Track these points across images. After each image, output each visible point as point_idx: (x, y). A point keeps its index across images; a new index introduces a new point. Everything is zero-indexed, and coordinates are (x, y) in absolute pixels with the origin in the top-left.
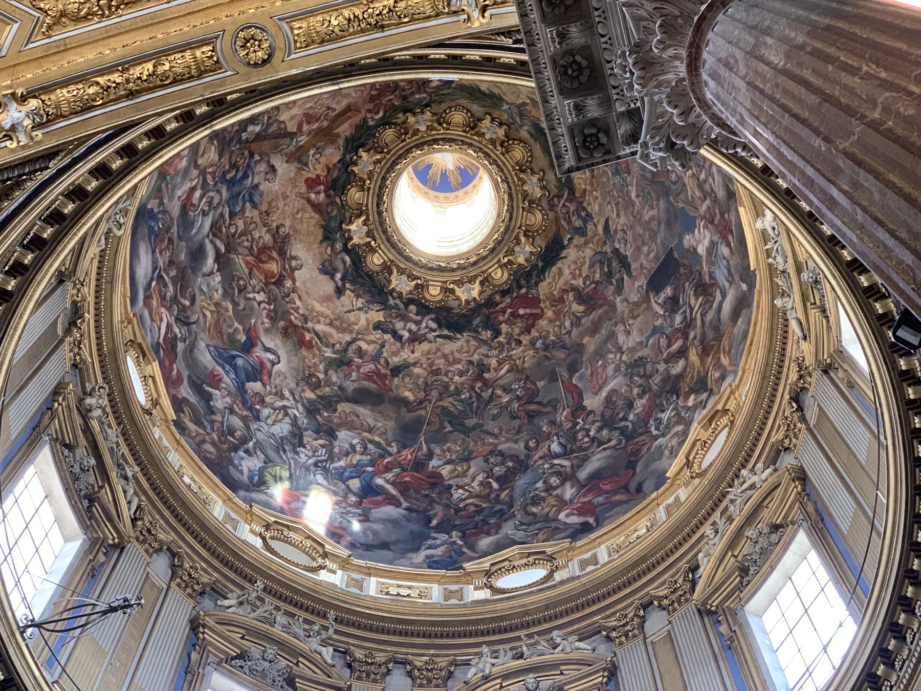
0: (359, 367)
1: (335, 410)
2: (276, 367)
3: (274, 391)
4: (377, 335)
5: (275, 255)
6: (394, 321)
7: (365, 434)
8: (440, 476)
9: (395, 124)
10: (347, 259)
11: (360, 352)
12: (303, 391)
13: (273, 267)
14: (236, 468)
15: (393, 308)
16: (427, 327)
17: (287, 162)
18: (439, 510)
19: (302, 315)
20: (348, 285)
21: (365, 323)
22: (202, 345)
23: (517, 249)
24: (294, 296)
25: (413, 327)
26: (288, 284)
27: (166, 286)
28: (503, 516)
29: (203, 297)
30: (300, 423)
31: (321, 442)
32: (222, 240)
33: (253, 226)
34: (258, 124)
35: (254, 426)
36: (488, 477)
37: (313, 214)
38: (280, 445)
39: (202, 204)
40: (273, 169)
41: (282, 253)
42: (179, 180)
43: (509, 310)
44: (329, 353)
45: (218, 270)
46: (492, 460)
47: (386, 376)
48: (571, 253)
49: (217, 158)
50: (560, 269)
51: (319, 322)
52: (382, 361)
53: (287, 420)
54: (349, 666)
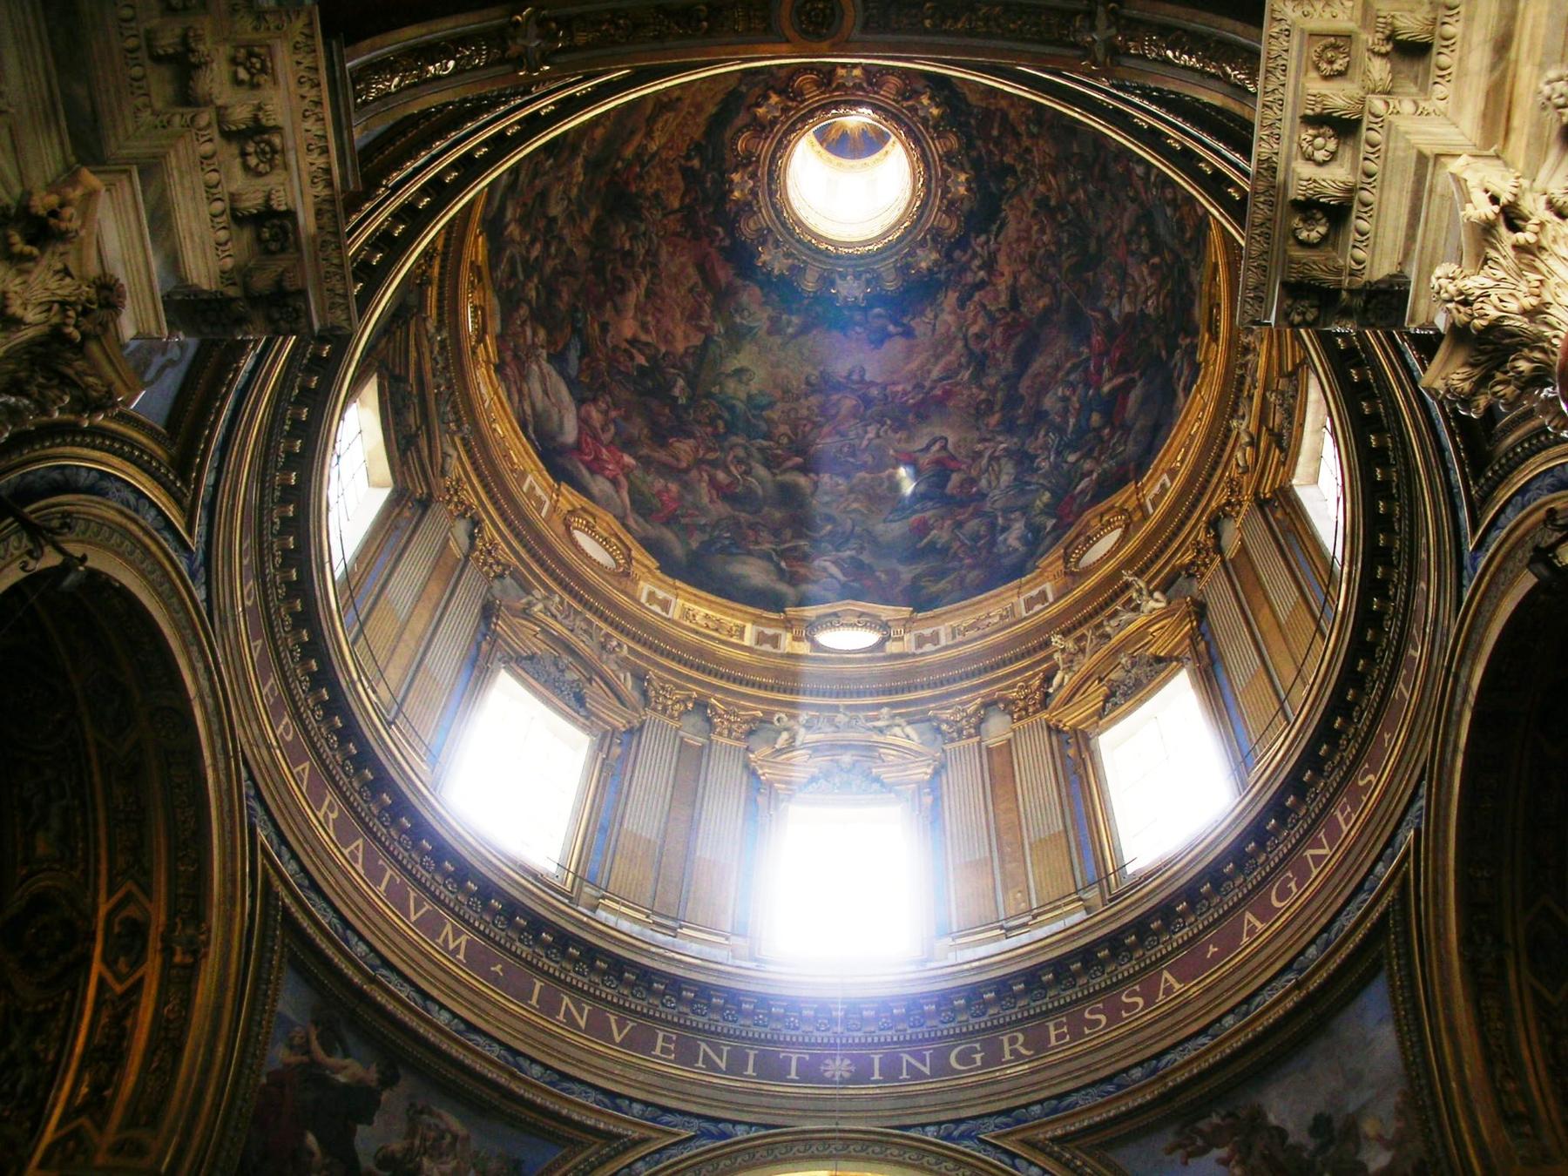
0: (994, 346)
1: (1022, 398)
2: (950, 446)
3: (969, 461)
4: (971, 306)
5: (835, 397)
7: (1060, 375)
8: (1129, 314)
9: (737, 214)
10: (877, 310)
11: (979, 337)
12: (987, 425)
13: (848, 403)
14: (1008, 554)
17: (738, 352)
18: (1156, 340)
19: (914, 388)
20: (905, 321)
22: (880, 528)
23: (921, 113)
24: (890, 389)
25: (977, 262)
26: (874, 392)
27: (795, 548)
28: (1184, 274)
29: (835, 505)
30: (1013, 448)
31: (1042, 433)
32: (788, 459)
33: (792, 416)
34: (676, 381)
35: (987, 507)
36: (1147, 262)
37: (811, 336)
38: (1020, 484)
39: (735, 472)
40: (740, 372)
41: (838, 387)
42: (689, 498)
43: (991, 146)
44: (966, 375)
45: (817, 474)
46: (1134, 247)
47: (1014, 318)
49: (692, 442)
51: (929, 372)
52: (997, 315)
53: (1003, 461)
54: (1191, 576)
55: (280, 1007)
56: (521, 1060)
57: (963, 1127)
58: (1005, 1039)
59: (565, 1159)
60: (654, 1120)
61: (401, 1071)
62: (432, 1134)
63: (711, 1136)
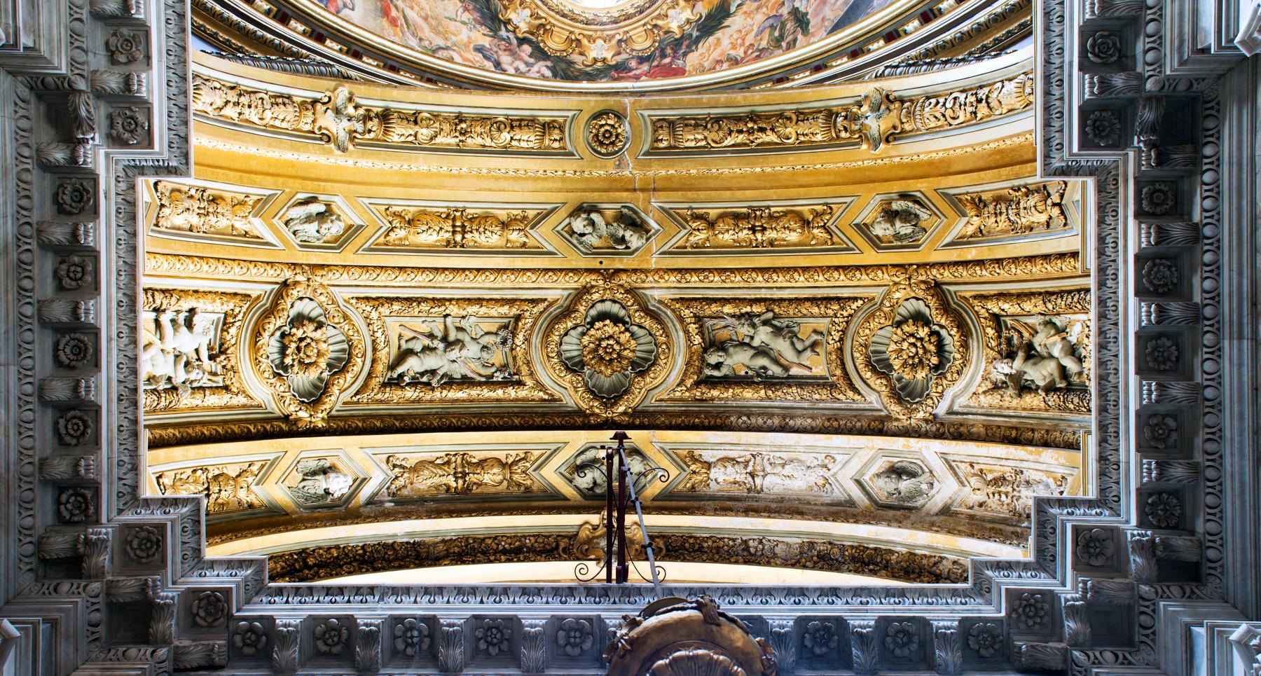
6: (500, 52)
15: (504, 40)
16: (538, 72)
21: (466, 40)
23: (671, 12)
25: (523, 67)
48: (736, 22)
50: (718, 39)
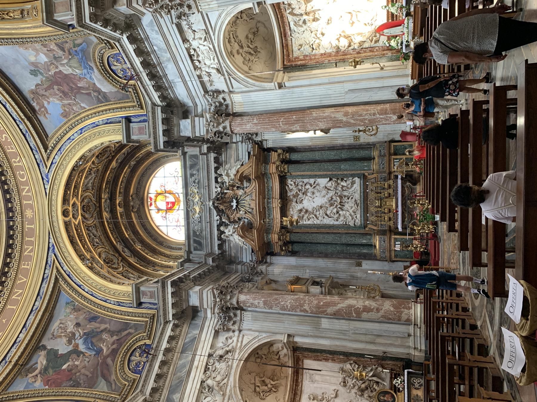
55: (22, 389)
56: (34, 309)
57: (44, 177)
58: (15, 164)
59: (65, 290)
60: (50, 266)
61: (41, 345)
62: (60, 330)
63: (54, 248)
